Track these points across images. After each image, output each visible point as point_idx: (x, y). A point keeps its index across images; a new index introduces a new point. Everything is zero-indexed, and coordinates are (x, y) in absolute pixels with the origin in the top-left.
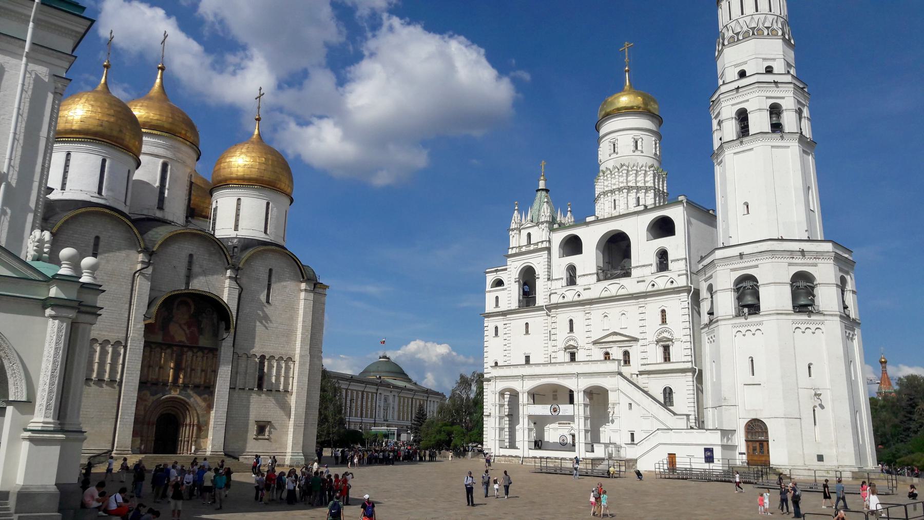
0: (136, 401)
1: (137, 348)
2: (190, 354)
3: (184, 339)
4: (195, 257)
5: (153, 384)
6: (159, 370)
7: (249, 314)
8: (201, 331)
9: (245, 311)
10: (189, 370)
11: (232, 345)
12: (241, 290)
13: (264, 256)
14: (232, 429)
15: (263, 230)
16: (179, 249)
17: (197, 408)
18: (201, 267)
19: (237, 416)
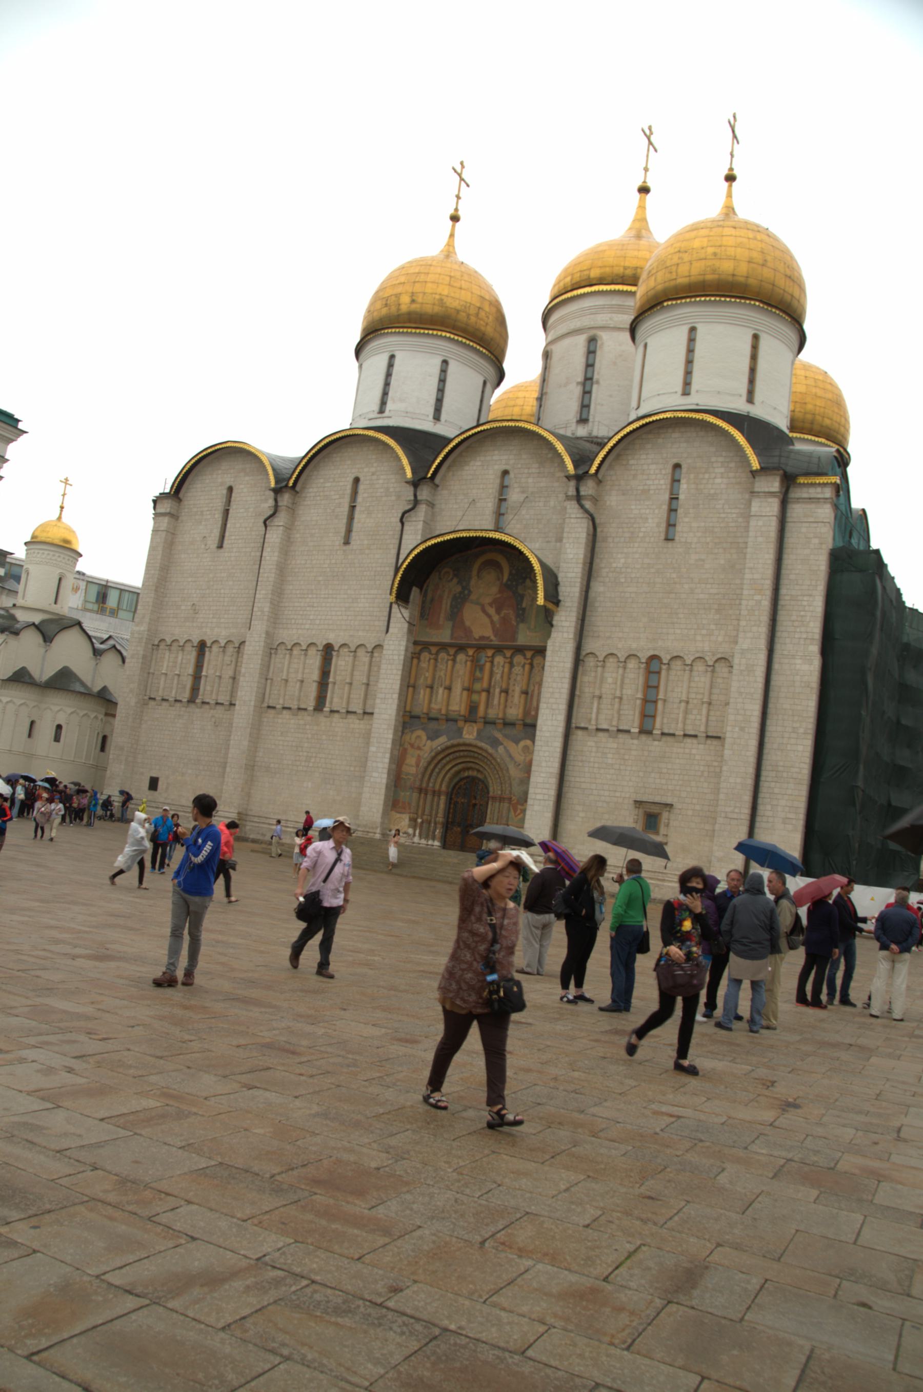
0: (389, 746)
1: (395, 652)
2: (499, 659)
3: (488, 632)
4: (512, 475)
5: (431, 719)
7: (623, 570)
8: (522, 615)
9: (614, 565)
10: (497, 690)
11: (571, 636)
13: (660, 441)
14: (581, 814)
15: (679, 388)
17: (511, 767)
18: (523, 492)
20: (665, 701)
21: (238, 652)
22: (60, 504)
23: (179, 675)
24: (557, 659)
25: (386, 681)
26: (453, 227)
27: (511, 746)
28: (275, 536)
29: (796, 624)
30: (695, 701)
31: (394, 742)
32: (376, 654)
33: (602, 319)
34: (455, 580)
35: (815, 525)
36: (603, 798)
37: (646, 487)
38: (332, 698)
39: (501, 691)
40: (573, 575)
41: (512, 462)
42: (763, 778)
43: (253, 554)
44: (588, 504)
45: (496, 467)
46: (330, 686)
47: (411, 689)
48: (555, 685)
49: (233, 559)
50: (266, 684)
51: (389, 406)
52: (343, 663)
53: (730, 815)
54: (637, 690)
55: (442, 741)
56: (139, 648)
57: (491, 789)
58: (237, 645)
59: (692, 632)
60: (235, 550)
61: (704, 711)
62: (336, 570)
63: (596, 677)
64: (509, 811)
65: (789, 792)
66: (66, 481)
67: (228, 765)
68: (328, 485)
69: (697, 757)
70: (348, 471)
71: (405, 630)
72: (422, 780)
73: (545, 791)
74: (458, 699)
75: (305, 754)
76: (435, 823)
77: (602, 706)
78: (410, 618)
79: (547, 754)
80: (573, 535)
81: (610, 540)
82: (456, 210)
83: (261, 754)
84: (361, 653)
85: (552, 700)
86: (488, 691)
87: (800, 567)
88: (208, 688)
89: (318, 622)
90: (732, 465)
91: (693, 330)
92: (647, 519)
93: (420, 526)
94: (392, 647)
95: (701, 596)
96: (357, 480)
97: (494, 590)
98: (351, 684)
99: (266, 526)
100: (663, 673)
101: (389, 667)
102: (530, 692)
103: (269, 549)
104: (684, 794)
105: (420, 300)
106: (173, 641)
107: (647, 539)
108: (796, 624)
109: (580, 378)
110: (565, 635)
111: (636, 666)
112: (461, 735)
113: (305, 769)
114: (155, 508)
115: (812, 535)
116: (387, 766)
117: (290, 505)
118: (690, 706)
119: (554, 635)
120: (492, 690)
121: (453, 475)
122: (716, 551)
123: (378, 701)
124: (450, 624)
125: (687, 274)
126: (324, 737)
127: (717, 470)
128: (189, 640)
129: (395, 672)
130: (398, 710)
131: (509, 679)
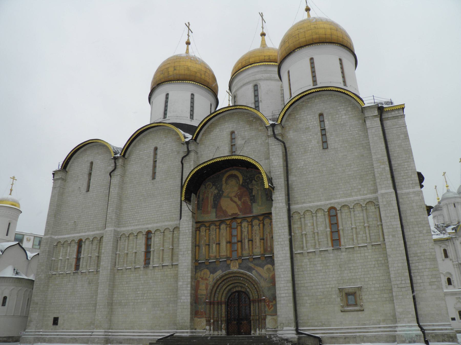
0: (189, 280)
2: (245, 224)
3: (237, 211)
4: (236, 133)
6: (216, 247)
7: (304, 167)
8: (253, 199)
9: (299, 166)
10: (246, 241)
11: (284, 204)
12: (282, 144)
13: (309, 105)
14: (309, 302)
16: (220, 131)
18: (243, 139)
19: (312, 284)
20: (343, 230)
21: (100, 242)
22: (11, 188)
23: (68, 259)
24: (279, 217)
25: (183, 245)
26: (188, 47)
27: (259, 269)
28: (116, 180)
29: (405, 177)
30: (360, 227)
31: (192, 278)
32: (175, 232)
33: (258, 76)
34: (214, 188)
35: (400, 128)
36: (319, 290)
37: (307, 126)
38: (153, 259)
39: (249, 241)
40: (279, 173)
41: (235, 126)
42: (410, 262)
43: (105, 192)
44: (280, 138)
45: (227, 130)
46: (152, 253)
47: (197, 248)
48: (280, 231)
49: (94, 196)
50: (116, 257)
51: (168, 114)
52: (158, 239)
53: (400, 286)
54: (326, 228)
55: (219, 273)
56: (46, 247)
57: (251, 296)
58: (99, 239)
59: (349, 191)
60: (95, 191)
61: (367, 231)
62: (149, 192)
63: (301, 224)
64: (265, 307)
65: (428, 266)
66: (13, 178)
67: (98, 304)
68: (141, 153)
69: (369, 257)
70: (151, 145)
71: (191, 216)
72: (210, 297)
73: (286, 291)
74: (225, 249)
75: (141, 292)
76: (221, 321)
77: (308, 239)
78: (192, 210)
79: (283, 270)
80: (275, 154)
81: (294, 154)
82: (188, 40)
83: (116, 296)
84: (167, 233)
85: (279, 240)
86: (241, 241)
87: (398, 149)
88: (85, 264)
89: (142, 220)
90: (349, 109)
91: (312, 59)
92: (311, 141)
93: (192, 163)
94: (185, 226)
95: (350, 173)
96: (156, 149)
97: (236, 189)
98: (163, 250)
99: (111, 176)
100: (339, 215)
101: (184, 237)
102: (265, 238)
103: (113, 187)
104: (367, 280)
105: (178, 69)
106: (65, 242)
107: (314, 150)
108: (405, 177)
109: (253, 101)
110: (281, 204)
111: (323, 214)
112: (230, 268)
113: (142, 301)
114: (53, 177)
115: (400, 134)
116: (189, 292)
117: (123, 165)
118: (358, 230)
119: (274, 205)
120: (243, 241)
121: (206, 138)
122: (352, 149)
123: (180, 256)
124: (214, 210)
125: (304, 37)
126: (151, 281)
127: (342, 113)
128: (73, 240)
129: (187, 239)
130: (192, 260)
131: (252, 233)
